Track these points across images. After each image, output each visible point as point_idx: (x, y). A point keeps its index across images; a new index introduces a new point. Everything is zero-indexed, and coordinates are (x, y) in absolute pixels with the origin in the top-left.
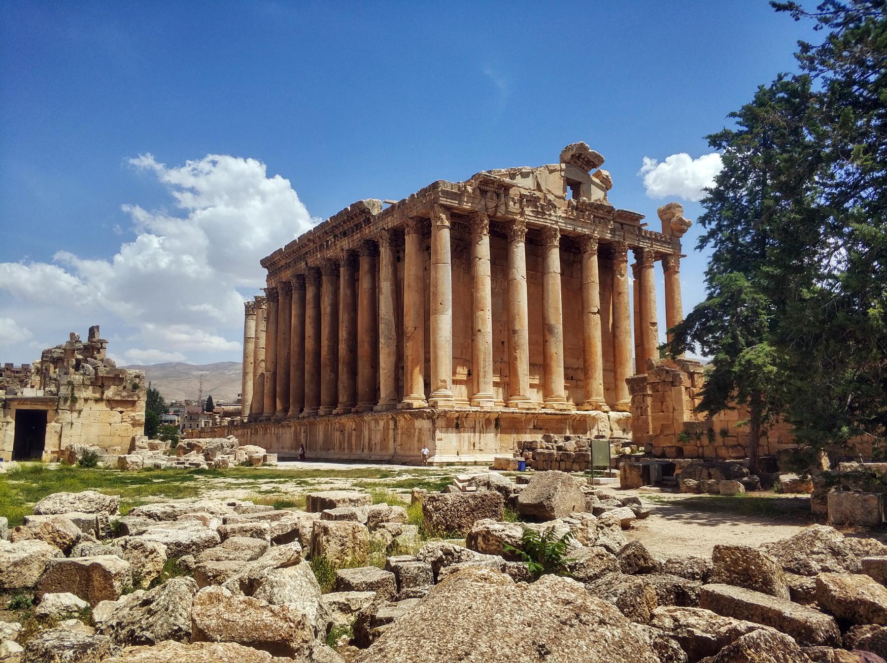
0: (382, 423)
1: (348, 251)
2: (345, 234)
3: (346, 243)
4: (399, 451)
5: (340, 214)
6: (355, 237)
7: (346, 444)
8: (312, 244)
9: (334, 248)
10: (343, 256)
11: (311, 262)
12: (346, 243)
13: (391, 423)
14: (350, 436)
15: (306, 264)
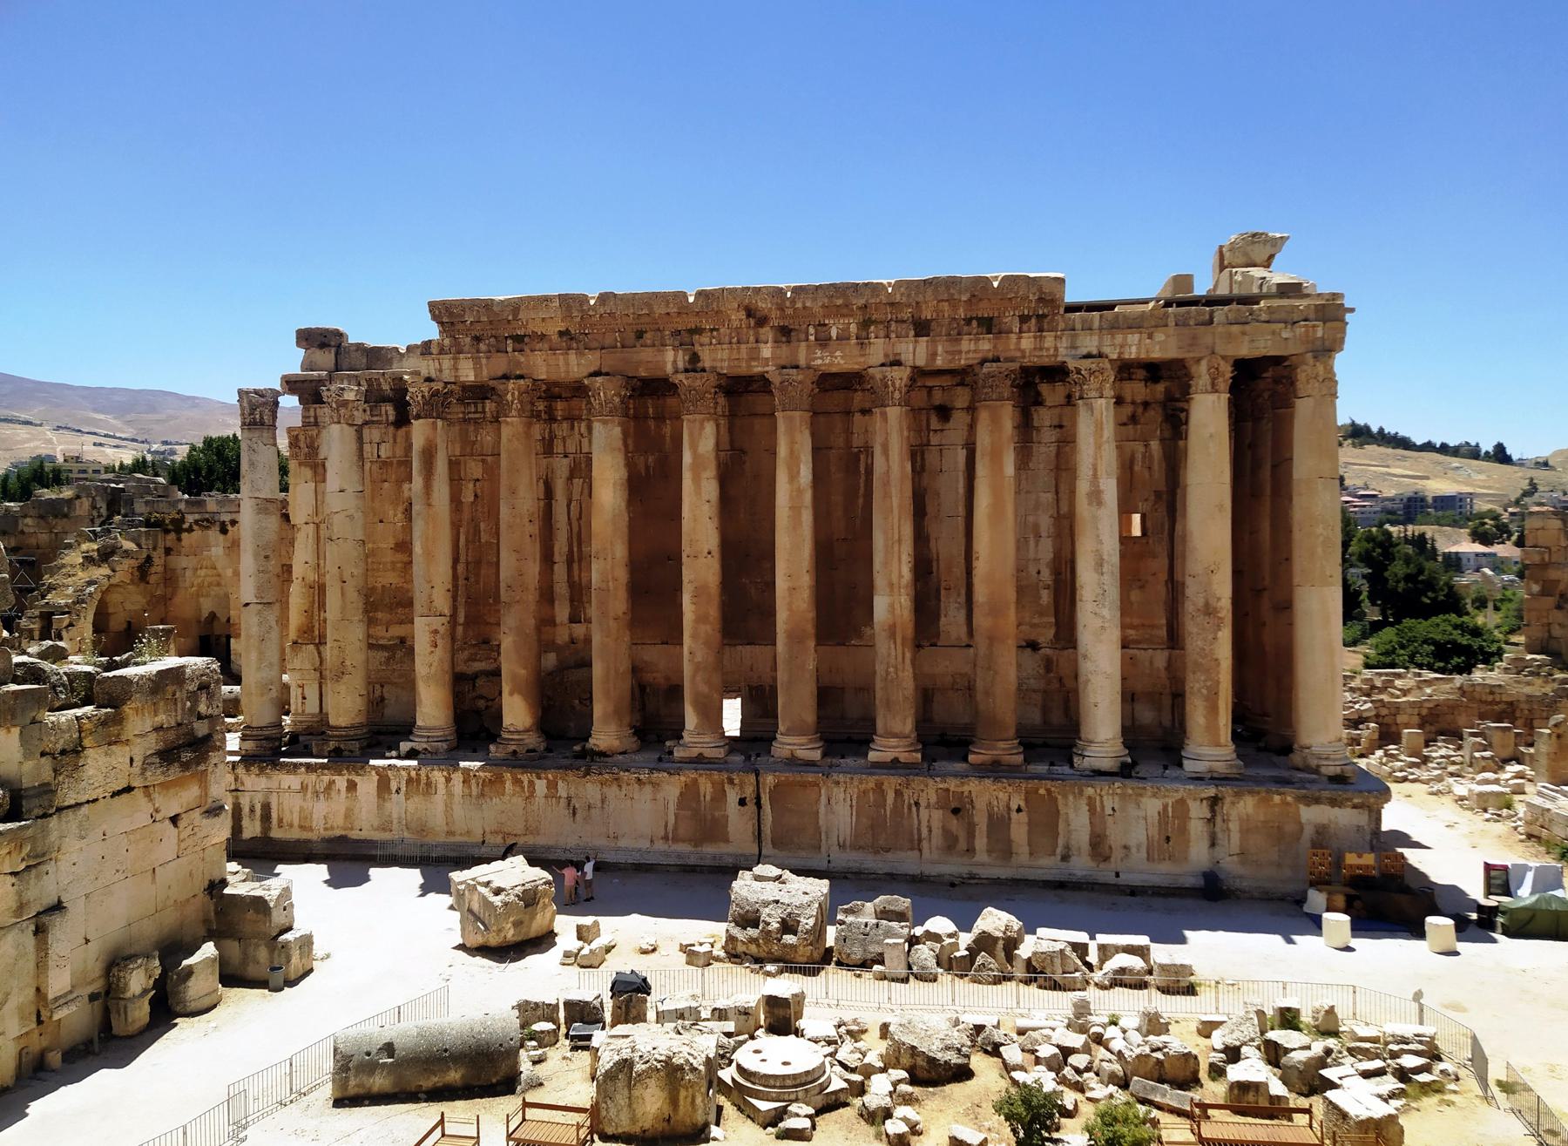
0: (1152, 806)
1: (914, 368)
2: (922, 328)
3: (915, 352)
4: (1230, 865)
5: (952, 282)
6: (966, 344)
7: (981, 842)
8: (742, 314)
9: (856, 351)
10: (900, 376)
11: (719, 357)
12: (915, 352)
13: (1198, 811)
14: (999, 824)
15: (695, 358)
